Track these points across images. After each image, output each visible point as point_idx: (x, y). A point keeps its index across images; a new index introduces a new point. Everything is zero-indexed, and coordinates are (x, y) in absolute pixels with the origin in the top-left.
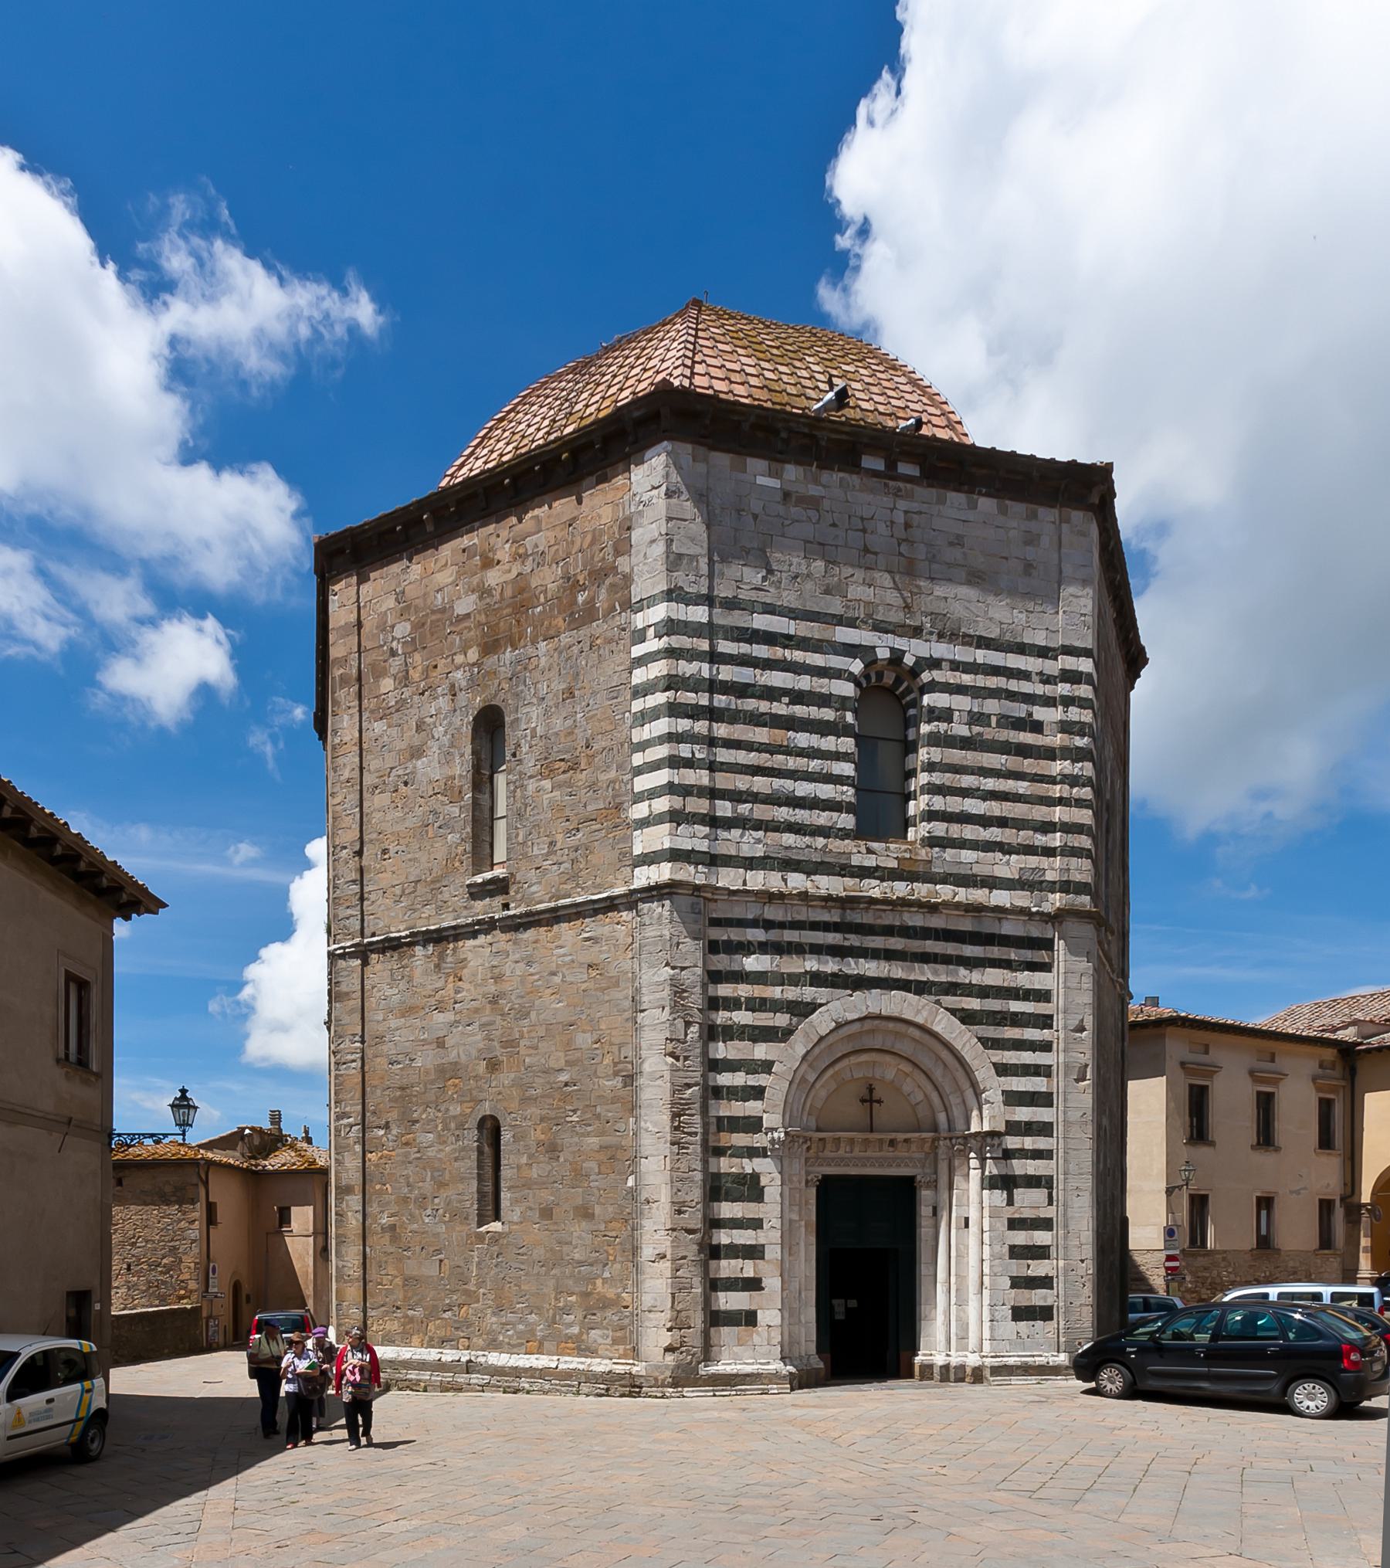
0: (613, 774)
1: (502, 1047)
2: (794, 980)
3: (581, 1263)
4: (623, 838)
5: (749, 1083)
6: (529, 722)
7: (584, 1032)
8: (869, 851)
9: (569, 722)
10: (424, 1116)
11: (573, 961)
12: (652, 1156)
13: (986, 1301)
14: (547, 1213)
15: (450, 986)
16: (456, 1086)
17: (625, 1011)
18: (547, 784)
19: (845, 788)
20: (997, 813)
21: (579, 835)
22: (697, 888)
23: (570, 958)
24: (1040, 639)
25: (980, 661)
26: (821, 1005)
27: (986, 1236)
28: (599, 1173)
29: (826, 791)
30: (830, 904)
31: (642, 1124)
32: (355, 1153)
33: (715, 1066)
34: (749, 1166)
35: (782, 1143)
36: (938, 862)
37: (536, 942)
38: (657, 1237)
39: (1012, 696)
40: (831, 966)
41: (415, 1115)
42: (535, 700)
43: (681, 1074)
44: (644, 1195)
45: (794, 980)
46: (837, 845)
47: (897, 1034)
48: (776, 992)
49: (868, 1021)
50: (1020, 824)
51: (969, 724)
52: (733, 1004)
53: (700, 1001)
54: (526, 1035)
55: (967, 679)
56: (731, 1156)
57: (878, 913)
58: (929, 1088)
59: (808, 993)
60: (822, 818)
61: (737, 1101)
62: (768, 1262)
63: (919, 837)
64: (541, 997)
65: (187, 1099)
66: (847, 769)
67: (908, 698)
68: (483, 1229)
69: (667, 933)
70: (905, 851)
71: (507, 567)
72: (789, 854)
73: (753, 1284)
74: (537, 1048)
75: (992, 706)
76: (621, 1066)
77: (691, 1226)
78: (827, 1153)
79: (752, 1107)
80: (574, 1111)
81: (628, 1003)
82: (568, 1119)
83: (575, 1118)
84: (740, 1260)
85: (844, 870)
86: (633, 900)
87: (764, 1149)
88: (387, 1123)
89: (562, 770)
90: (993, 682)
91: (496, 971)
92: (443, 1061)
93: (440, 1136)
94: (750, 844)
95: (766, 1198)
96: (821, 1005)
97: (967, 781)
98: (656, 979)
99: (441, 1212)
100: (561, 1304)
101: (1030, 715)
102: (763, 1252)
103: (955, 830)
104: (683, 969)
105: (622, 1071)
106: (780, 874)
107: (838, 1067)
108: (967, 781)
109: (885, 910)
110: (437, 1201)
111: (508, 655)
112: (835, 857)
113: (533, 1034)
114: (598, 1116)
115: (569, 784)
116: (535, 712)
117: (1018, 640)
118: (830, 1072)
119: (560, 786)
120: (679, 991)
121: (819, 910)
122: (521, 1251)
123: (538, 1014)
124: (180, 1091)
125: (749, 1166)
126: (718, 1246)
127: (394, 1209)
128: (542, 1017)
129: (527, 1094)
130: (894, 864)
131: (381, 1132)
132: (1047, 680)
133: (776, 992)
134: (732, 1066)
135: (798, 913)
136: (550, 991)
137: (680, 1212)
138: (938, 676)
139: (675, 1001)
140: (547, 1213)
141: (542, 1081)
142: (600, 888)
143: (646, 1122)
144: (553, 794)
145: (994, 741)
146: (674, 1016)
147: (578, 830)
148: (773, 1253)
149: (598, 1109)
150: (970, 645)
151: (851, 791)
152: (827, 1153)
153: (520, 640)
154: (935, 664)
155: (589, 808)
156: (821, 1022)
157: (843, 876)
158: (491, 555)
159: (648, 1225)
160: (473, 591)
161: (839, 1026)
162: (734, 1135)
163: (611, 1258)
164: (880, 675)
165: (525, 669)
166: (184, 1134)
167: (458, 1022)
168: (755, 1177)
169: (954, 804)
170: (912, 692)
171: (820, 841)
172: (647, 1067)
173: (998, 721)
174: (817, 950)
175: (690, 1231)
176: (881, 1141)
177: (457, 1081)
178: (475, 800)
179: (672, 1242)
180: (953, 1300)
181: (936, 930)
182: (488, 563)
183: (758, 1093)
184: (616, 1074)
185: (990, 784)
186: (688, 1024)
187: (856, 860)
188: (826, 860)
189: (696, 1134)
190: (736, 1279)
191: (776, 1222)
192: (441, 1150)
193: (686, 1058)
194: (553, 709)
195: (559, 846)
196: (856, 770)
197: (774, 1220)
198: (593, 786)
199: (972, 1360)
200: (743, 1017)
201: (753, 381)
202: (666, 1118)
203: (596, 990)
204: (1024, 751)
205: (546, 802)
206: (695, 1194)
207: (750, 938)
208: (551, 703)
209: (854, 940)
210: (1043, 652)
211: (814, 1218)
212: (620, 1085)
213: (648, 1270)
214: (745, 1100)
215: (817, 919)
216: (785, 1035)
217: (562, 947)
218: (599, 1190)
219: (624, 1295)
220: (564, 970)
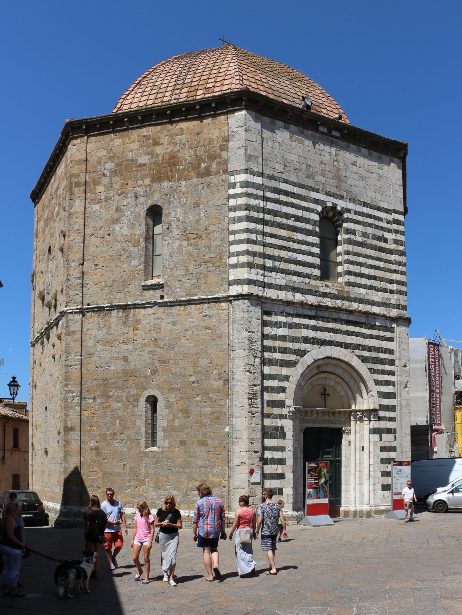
0: (218, 243)
1: (160, 363)
2: (296, 340)
3: (201, 467)
4: (224, 271)
5: (280, 385)
6: (176, 214)
7: (203, 358)
8: (326, 286)
9: (196, 217)
10: (116, 394)
11: (198, 325)
12: (239, 417)
13: (372, 482)
14: (183, 443)
15: (131, 332)
16: (134, 381)
17: (224, 350)
18: (185, 243)
19: (316, 258)
20: (373, 274)
21: (201, 268)
22: (258, 297)
23: (196, 323)
24: (386, 206)
25: (365, 212)
26: (308, 352)
27: (371, 454)
28: (211, 425)
29: (309, 259)
30: (312, 307)
31: (234, 402)
32: (76, 411)
33: (264, 377)
34: (280, 423)
35: (293, 412)
36: (352, 293)
37: (178, 315)
38: (241, 454)
39: (376, 227)
40: (311, 334)
41: (111, 393)
42: (179, 206)
43: (253, 380)
44: (235, 435)
45: (296, 340)
46: (314, 283)
47: (336, 365)
48: (290, 345)
49: (326, 359)
50: (381, 279)
51: (362, 237)
52: (272, 349)
53: (260, 348)
54: (173, 358)
55: (360, 218)
56: (273, 418)
57: (330, 313)
58: (348, 389)
59: (303, 346)
60: (308, 270)
61: (275, 393)
62: (288, 466)
63: (344, 281)
64: (181, 341)
65: (16, 382)
66: (317, 250)
67: (338, 223)
68: (148, 450)
69: (246, 316)
70: (340, 287)
71: (166, 147)
72: (295, 285)
73: (281, 476)
74: (178, 364)
75: (370, 230)
76: (222, 375)
77: (256, 450)
78: (308, 418)
79: (280, 396)
80: (198, 395)
81: (226, 347)
82: (195, 399)
83: (198, 398)
84: (276, 465)
85: (316, 293)
86: (229, 299)
87: (286, 415)
88: (95, 396)
89: (193, 238)
90: (370, 221)
91: (157, 327)
92: (127, 368)
93: (124, 404)
94: (280, 279)
95: (287, 437)
96: (308, 352)
97: (362, 260)
98: (241, 336)
99: (125, 441)
100: (190, 486)
101: (383, 235)
102: (285, 462)
103: (359, 280)
104: (253, 332)
105: (223, 377)
106: (292, 293)
107: (312, 379)
108: (362, 260)
109: (333, 312)
110: (122, 436)
111: (166, 184)
112: (313, 287)
113: (176, 358)
114: (210, 398)
115: (196, 244)
116: (179, 211)
117: (378, 205)
118: (309, 382)
119: (192, 245)
120: (252, 342)
121: (307, 310)
122: (169, 461)
123: (179, 349)
124: (13, 378)
125: (280, 423)
126: (267, 459)
127: (98, 439)
128: (181, 350)
129: (173, 386)
130: (335, 292)
131: (91, 401)
133: (290, 345)
134: (272, 377)
135: (299, 311)
136: (186, 338)
137: (251, 443)
139: (250, 347)
140: (183, 443)
141: (180, 380)
142: (212, 293)
143: (236, 401)
144: (188, 248)
145: (371, 245)
146: (250, 354)
147: (201, 266)
148: (290, 462)
149: (211, 395)
150: (361, 205)
151: (319, 260)
152: (308, 418)
153: (172, 179)
154: (349, 211)
155: (207, 256)
156: (308, 360)
157: (317, 296)
158: (158, 140)
159: (237, 449)
160: (148, 154)
161: (315, 361)
162: (274, 409)
163: (217, 464)
164: (327, 213)
165: (174, 191)
166: (13, 399)
167: (136, 349)
168: (282, 428)
169: (358, 269)
170: (339, 221)
171: (307, 280)
172: (236, 376)
173: (372, 237)
174: (307, 327)
175: (256, 452)
176: (329, 412)
177: (134, 378)
178: (146, 247)
179: (249, 456)
180: (358, 482)
181: (352, 321)
182: (156, 143)
183: (283, 390)
184: (220, 379)
185: (370, 262)
186: (255, 357)
187: (321, 290)
188: (310, 288)
189: (258, 407)
190: (275, 474)
191: (291, 448)
192: (126, 411)
193: (254, 373)
194: (188, 211)
195: (190, 272)
196: (320, 251)
197: (290, 447)
198: (208, 247)
199: (366, 508)
200: (277, 356)
201: (266, 85)
202: (246, 401)
203: (210, 339)
204: (381, 250)
205: (184, 252)
206: (259, 435)
207: (280, 320)
208: (188, 208)
209: (321, 324)
210: (387, 211)
211: (302, 447)
212: (222, 384)
213: (236, 470)
214: (278, 393)
215: (307, 314)
217: (191, 318)
218: (211, 432)
219: (223, 481)
220: (193, 329)
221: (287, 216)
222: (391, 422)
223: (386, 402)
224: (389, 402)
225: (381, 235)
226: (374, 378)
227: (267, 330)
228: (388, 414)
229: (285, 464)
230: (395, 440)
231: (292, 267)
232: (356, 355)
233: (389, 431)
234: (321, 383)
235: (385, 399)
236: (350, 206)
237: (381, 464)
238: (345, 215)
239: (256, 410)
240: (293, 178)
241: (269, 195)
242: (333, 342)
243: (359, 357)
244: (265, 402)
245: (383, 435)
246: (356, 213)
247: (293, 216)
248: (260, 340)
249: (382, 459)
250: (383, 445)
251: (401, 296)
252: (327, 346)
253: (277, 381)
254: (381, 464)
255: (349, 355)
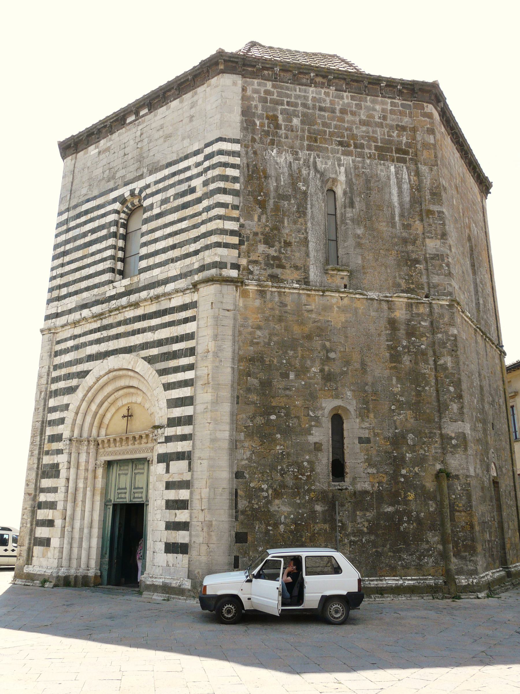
8: (114, 287)
26: (90, 371)
77: (30, 492)
96: (90, 371)
101: (189, 186)
102: (56, 505)
132: (198, 165)
138: (149, 191)
164: (133, 204)
171: (96, 291)
190: (46, 520)
209: (105, 333)
216: (71, 390)
221: (85, 235)
222: (184, 443)
223: (178, 412)
224: (183, 411)
225: (186, 188)
226: (164, 381)
227: (58, 360)
228: (180, 430)
229: (56, 509)
230: (190, 469)
231: (83, 285)
232: (142, 358)
233: (180, 456)
234: (126, 403)
235: (178, 409)
236: (150, 179)
237: (166, 509)
238: (143, 195)
239: (35, 447)
240: (96, 193)
241: (72, 224)
242: (116, 350)
243: (145, 359)
244: (47, 437)
245: (171, 463)
246: (157, 182)
247: (89, 231)
248: (46, 374)
249: (167, 502)
250: (171, 480)
251: (207, 252)
252: (109, 357)
253: (58, 412)
254: (166, 509)
255: (133, 360)
